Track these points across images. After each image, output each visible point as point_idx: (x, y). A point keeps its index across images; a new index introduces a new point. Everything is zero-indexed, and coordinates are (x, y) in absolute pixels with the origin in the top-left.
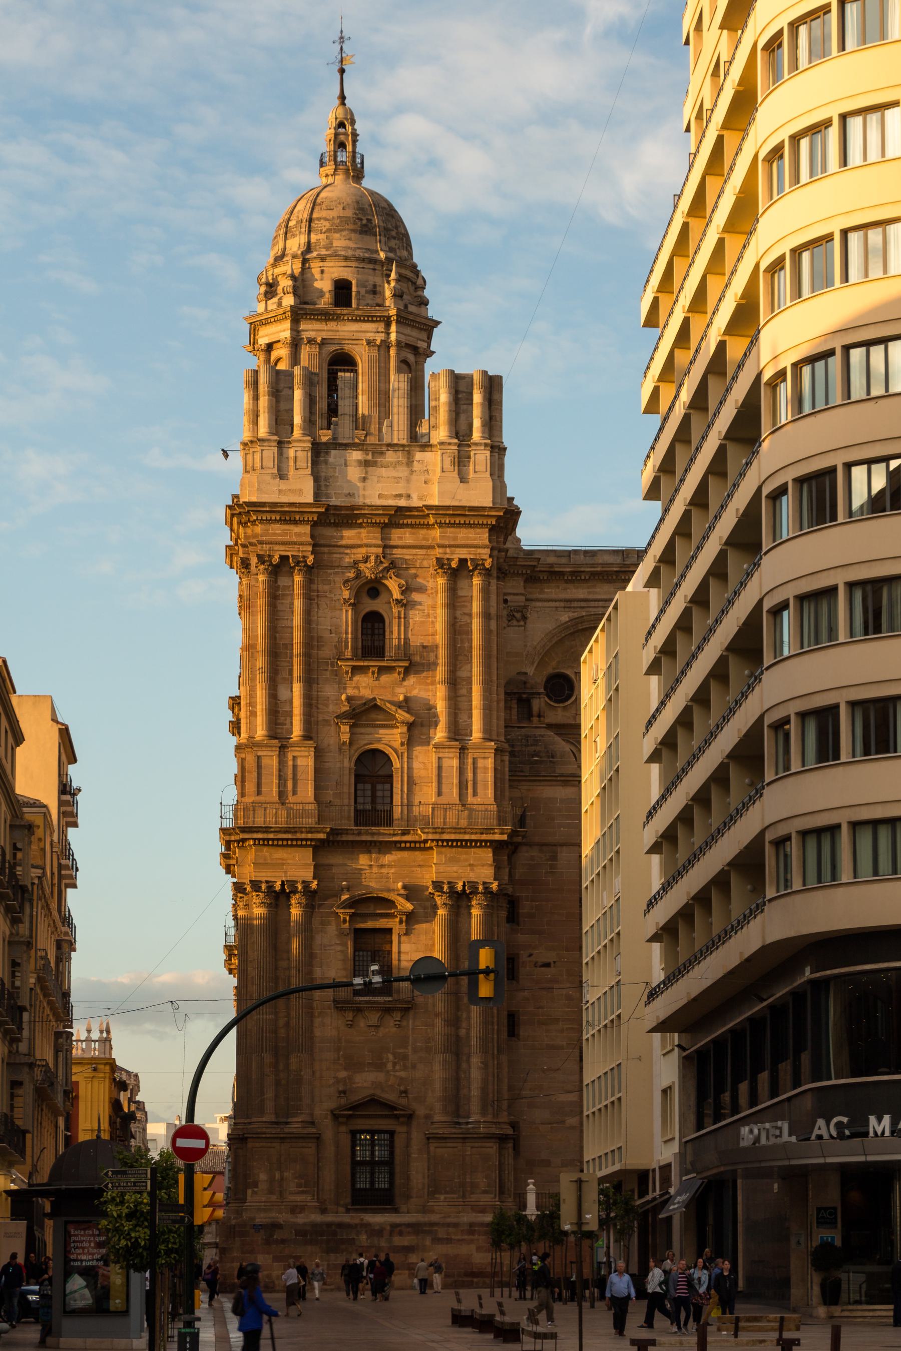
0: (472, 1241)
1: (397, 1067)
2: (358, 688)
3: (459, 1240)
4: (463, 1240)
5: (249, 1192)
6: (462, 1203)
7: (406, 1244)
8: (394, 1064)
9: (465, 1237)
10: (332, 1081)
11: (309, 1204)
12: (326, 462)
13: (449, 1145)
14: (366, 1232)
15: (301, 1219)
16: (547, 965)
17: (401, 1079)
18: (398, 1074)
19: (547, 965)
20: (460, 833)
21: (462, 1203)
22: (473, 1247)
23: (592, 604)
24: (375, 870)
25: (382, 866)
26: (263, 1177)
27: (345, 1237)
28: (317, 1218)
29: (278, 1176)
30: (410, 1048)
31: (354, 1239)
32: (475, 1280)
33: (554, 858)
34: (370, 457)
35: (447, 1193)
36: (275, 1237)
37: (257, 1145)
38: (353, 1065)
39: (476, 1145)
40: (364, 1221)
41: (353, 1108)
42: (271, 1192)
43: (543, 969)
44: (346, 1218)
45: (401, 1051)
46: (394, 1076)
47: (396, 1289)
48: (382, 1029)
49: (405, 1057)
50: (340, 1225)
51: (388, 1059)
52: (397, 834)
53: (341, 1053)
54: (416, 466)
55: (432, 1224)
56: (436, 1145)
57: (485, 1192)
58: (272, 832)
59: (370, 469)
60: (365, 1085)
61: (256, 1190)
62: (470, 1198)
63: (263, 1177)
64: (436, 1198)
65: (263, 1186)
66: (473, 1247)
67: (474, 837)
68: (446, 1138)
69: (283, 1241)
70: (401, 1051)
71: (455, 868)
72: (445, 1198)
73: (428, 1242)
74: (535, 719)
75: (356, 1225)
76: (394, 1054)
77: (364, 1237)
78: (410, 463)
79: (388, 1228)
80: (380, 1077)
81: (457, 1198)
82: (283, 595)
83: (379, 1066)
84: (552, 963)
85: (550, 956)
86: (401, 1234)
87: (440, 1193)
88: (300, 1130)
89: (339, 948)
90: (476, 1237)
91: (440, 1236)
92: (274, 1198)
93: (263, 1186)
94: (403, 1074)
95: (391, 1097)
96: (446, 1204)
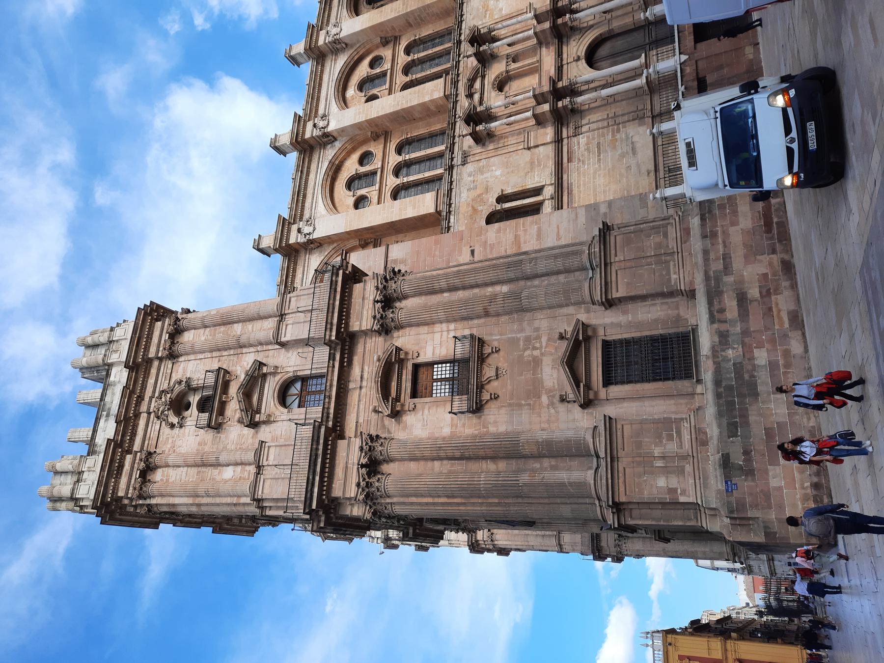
0: (726, 234)
1: (538, 345)
3: (725, 246)
4: (724, 242)
5: (682, 499)
6: (680, 255)
7: (735, 303)
8: (535, 348)
9: (720, 240)
10: (552, 411)
11: (693, 424)
13: (614, 278)
14: (723, 350)
15: (713, 431)
16: (473, 252)
17: (549, 340)
18: (544, 344)
20: (333, 308)
21: (680, 255)
22: (732, 230)
26: (662, 482)
27: (733, 375)
29: (659, 463)
30: (518, 336)
31: (734, 364)
32: (775, 220)
34: (105, 413)
35: (669, 274)
36: (741, 463)
37: (622, 489)
38: (534, 390)
39: (613, 252)
40: (710, 353)
44: (708, 375)
45: (521, 343)
46: (546, 348)
47: (800, 307)
48: (500, 365)
49: (528, 339)
50: (717, 383)
51: (529, 355)
52: (333, 364)
53: (523, 402)
55: (707, 278)
56: (614, 290)
57: (666, 235)
58: (314, 479)
60: (555, 375)
61: (679, 491)
62: (673, 248)
63: (662, 482)
64: (676, 283)
65: (674, 482)
66: (732, 230)
67: (338, 297)
68: (606, 283)
69: (747, 453)
70: (521, 343)
72: (675, 273)
73: (730, 279)
75: (714, 363)
76: (525, 350)
77: (730, 352)
79: (716, 326)
81: (674, 261)
82: (167, 476)
83: (536, 363)
84: (471, 249)
86: (722, 311)
87: (669, 280)
88: (603, 439)
89: (426, 411)
90: (719, 229)
91: (721, 267)
92: (688, 468)
93: (674, 482)
94: (544, 340)
95: (564, 345)
96: (681, 271)
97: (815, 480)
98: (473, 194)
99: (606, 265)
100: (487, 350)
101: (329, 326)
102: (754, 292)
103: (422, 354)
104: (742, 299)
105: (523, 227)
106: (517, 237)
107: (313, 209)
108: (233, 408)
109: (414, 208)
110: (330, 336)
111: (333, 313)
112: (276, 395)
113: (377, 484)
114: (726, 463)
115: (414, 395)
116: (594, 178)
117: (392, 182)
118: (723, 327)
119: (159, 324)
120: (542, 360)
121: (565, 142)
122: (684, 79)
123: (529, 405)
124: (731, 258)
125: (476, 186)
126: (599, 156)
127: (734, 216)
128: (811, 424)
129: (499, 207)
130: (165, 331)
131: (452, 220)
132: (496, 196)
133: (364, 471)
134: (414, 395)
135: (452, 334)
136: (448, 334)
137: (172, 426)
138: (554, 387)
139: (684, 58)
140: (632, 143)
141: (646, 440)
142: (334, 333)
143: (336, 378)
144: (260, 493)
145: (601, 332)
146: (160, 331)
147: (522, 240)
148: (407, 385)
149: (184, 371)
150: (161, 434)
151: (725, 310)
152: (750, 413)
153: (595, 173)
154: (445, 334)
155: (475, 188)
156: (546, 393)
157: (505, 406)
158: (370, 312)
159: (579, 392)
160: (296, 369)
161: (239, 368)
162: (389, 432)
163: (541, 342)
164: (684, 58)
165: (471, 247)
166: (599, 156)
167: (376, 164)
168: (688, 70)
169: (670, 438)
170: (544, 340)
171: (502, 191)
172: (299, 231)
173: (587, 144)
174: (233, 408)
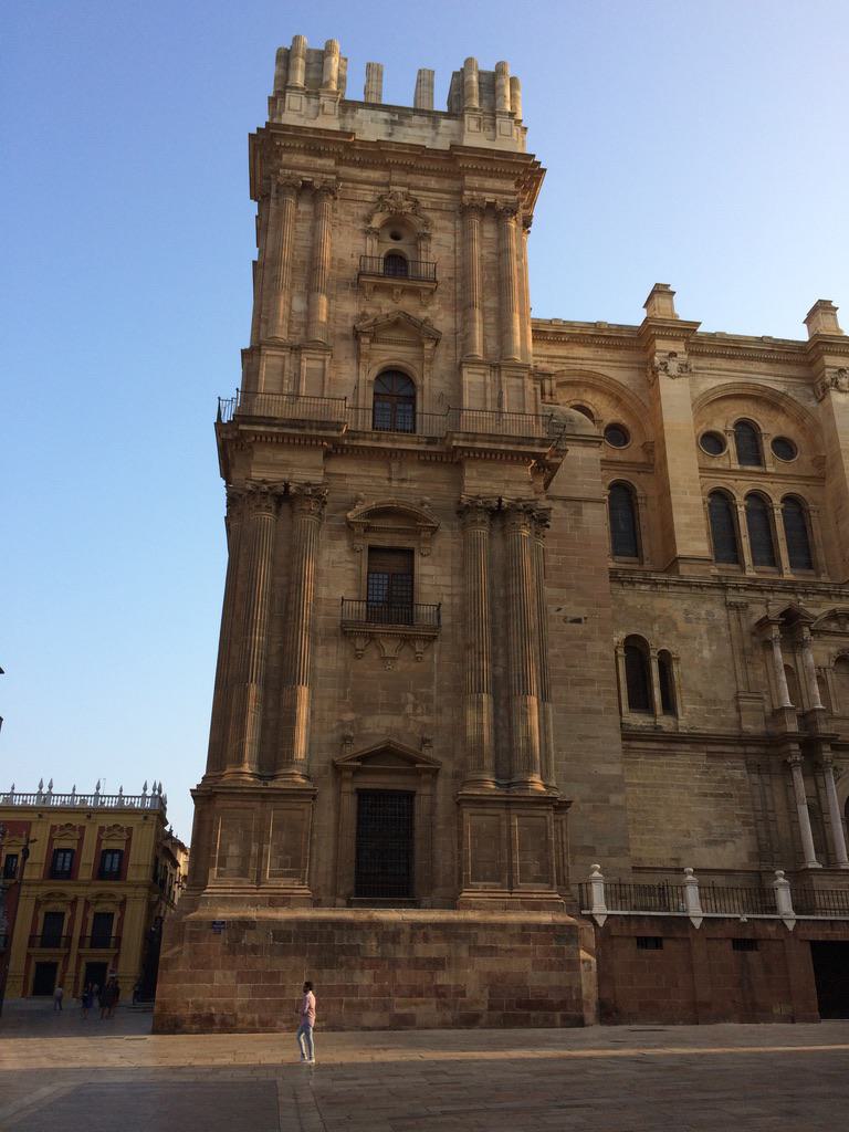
0: (525, 953)
1: (419, 711)
2: (380, 308)
3: (508, 951)
4: (512, 950)
6: (509, 895)
7: (434, 955)
8: (415, 707)
9: (516, 946)
12: (353, 118)
13: (488, 811)
14: (376, 934)
15: (283, 914)
16: (578, 621)
18: (419, 719)
19: (578, 621)
20: (495, 442)
21: (509, 895)
22: (528, 961)
23: (571, 361)
24: (395, 484)
25: (403, 480)
27: (345, 943)
28: (306, 914)
29: (254, 849)
32: (533, 1014)
33: (579, 512)
34: (396, 118)
37: (230, 804)
38: (363, 705)
39: (523, 812)
41: (364, 758)
42: (243, 873)
43: (574, 625)
44: (348, 914)
47: (418, 1028)
48: (399, 662)
49: (428, 699)
52: (422, 443)
54: (441, 130)
56: (473, 811)
58: (275, 425)
59: (395, 127)
60: (378, 731)
63: (234, 850)
65: (232, 864)
66: (528, 961)
67: (511, 448)
68: (483, 802)
69: (254, 949)
71: (488, 484)
73: (464, 954)
74: (548, 398)
76: (415, 695)
78: (435, 127)
79: (407, 929)
80: (397, 722)
81: (502, 888)
83: (396, 708)
85: (581, 612)
86: (426, 939)
89: (351, 566)
91: (481, 943)
92: (246, 882)
94: (426, 719)
95: (409, 745)
97: (217, 1019)
98: (679, 617)
99: (508, 803)
100: (419, 647)
101: (470, 437)
102: (443, 978)
103: (425, 559)
104: (437, 964)
105: (604, 692)
106: (592, 681)
107: (709, 371)
108: (384, 306)
109: (687, 525)
110: (458, 439)
111: (489, 441)
112: (394, 362)
113: (264, 505)
114: (245, 924)
115: (372, 550)
116: (679, 787)
117: (740, 489)
118: (404, 938)
119: (511, 186)
120: (400, 715)
121: (740, 749)
122: (759, 923)
123: (345, 698)
124: (491, 956)
125: (691, 622)
126: (711, 795)
127: (546, 967)
128: (279, 1023)
129: (653, 654)
130: (499, 196)
131: (643, 587)
132: (671, 649)
133: (281, 489)
134: (372, 550)
135: (446, 600)
136: (447, 595)
137: (368, 220)
138: (365, 729)
139: (790, 925)
140: (725, 842)
141: (284, 836)
142: (461, 444)
143: (403, 446)
144: (268, 352)
145: (426, 790)
146: (494, 189)
147: (587, 689)
148: (386, 541)
149: (443, 229)
150: (360, 204)
151: (426, 942)
152: (299, 958)
153: (686, 788)
154: (449, 591)
155: (688, 621)
156: (356, 719)
157: (346, 666)
158: (488, 490)
159: (351, 760)
160: (426, 387)
161: (436, 307)
162: (329, 518)
163: (423, 714)
164: (790, 925)
165: (586, 618)
166: (711, 795)
167: (772, 463)
168: (771, 929)
169: (284, 864)
170: (426, 719)
171: (678, 659)
172: (673, 354)
173: (732, 780)
174: (384, 306)
